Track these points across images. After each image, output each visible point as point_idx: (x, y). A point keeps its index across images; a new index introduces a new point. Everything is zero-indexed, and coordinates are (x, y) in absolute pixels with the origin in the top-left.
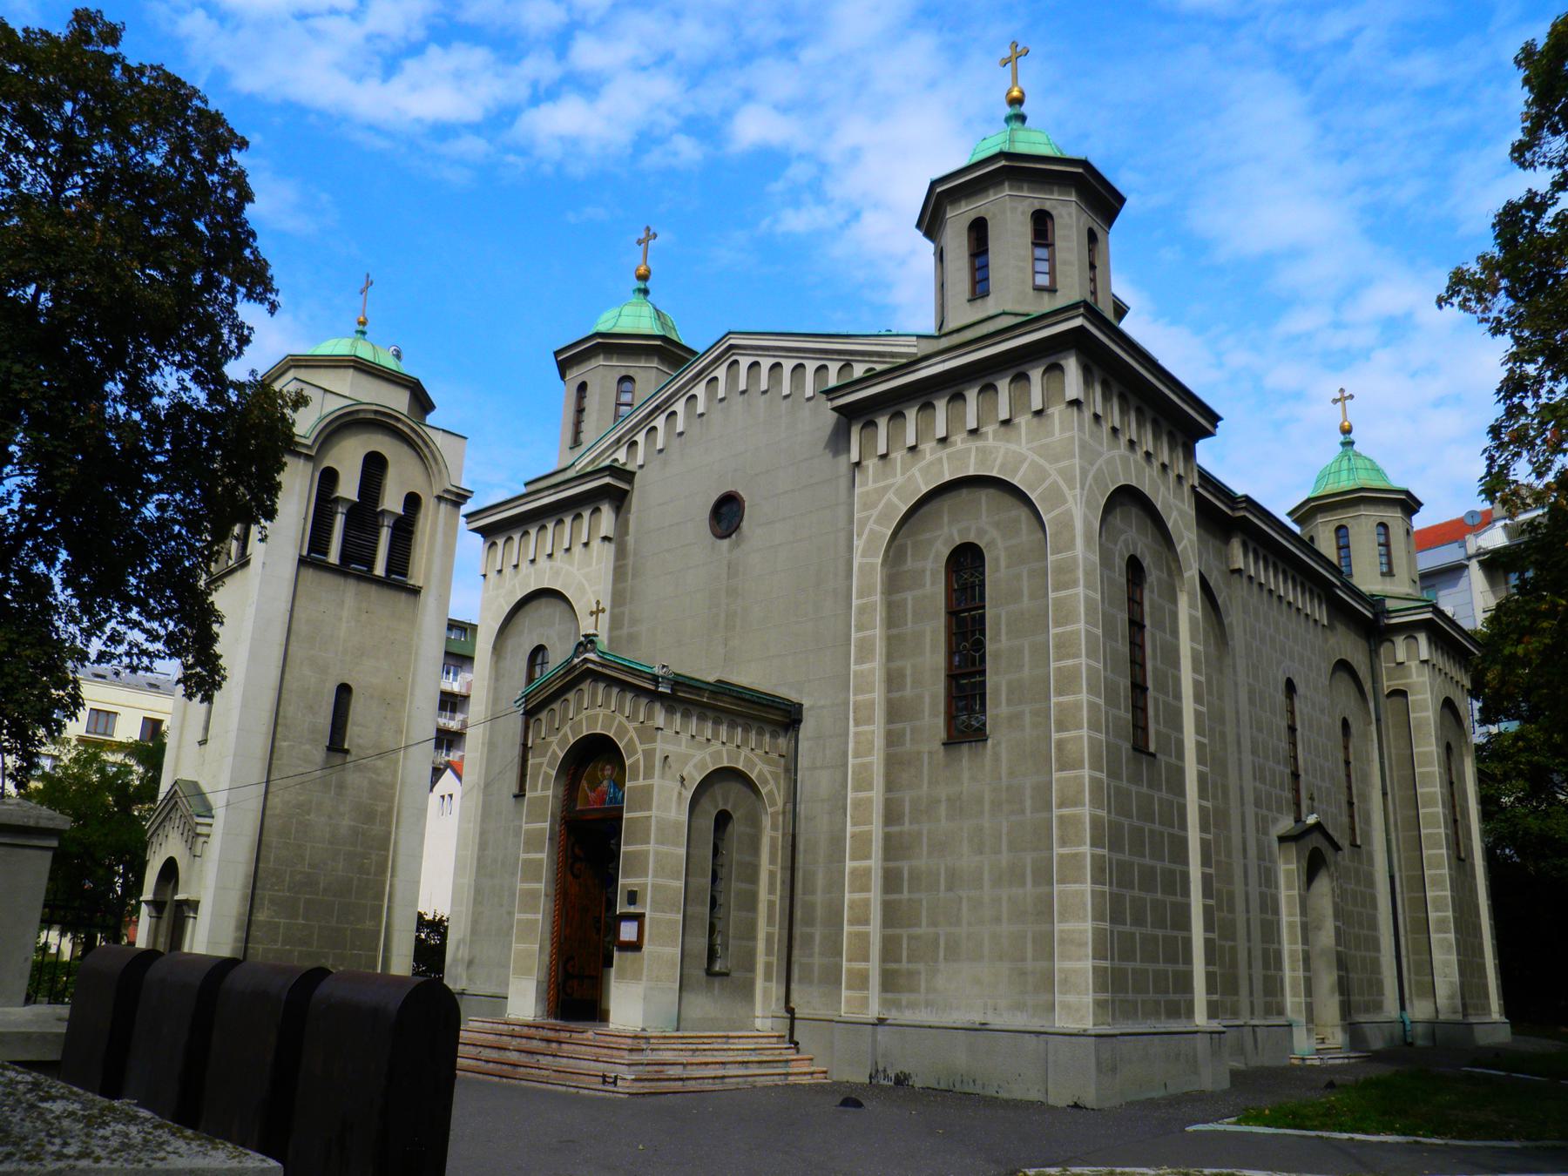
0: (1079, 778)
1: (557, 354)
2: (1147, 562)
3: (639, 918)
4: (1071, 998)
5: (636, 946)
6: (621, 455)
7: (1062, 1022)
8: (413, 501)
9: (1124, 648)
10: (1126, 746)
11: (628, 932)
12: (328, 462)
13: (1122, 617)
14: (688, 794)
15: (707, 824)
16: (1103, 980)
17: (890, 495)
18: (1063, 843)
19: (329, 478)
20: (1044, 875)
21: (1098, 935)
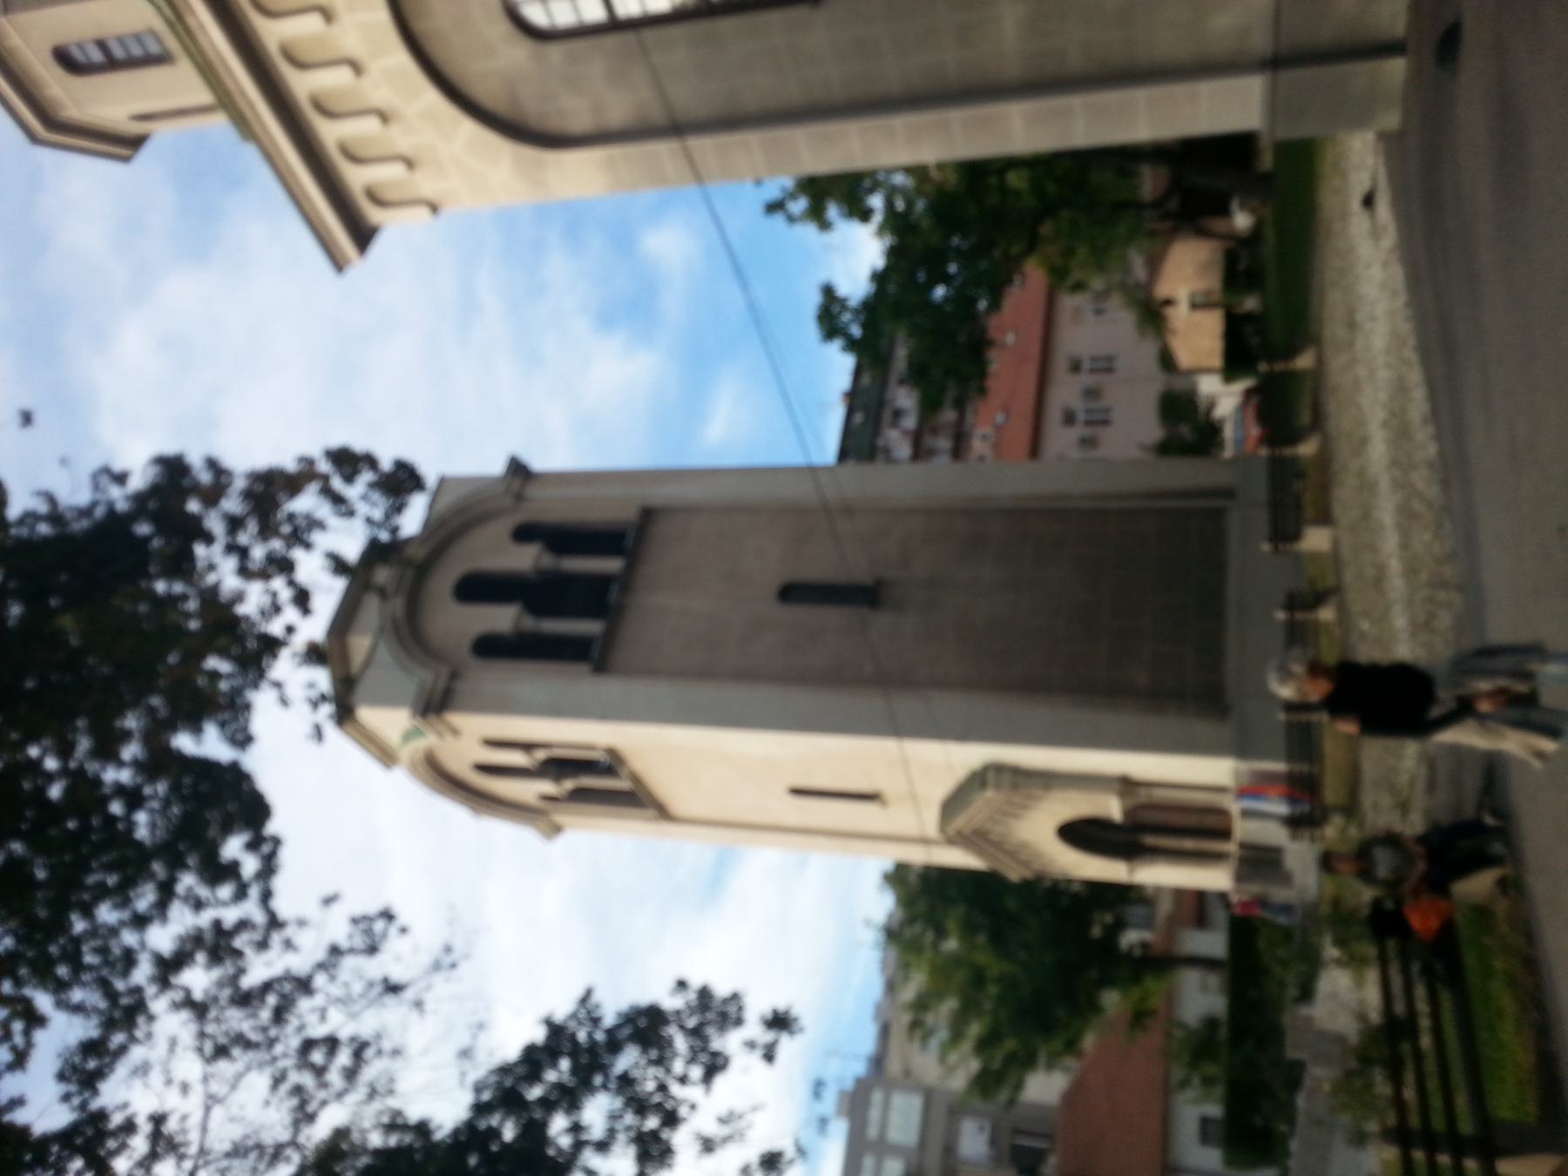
8: (524, 534)
19: (490, 647)
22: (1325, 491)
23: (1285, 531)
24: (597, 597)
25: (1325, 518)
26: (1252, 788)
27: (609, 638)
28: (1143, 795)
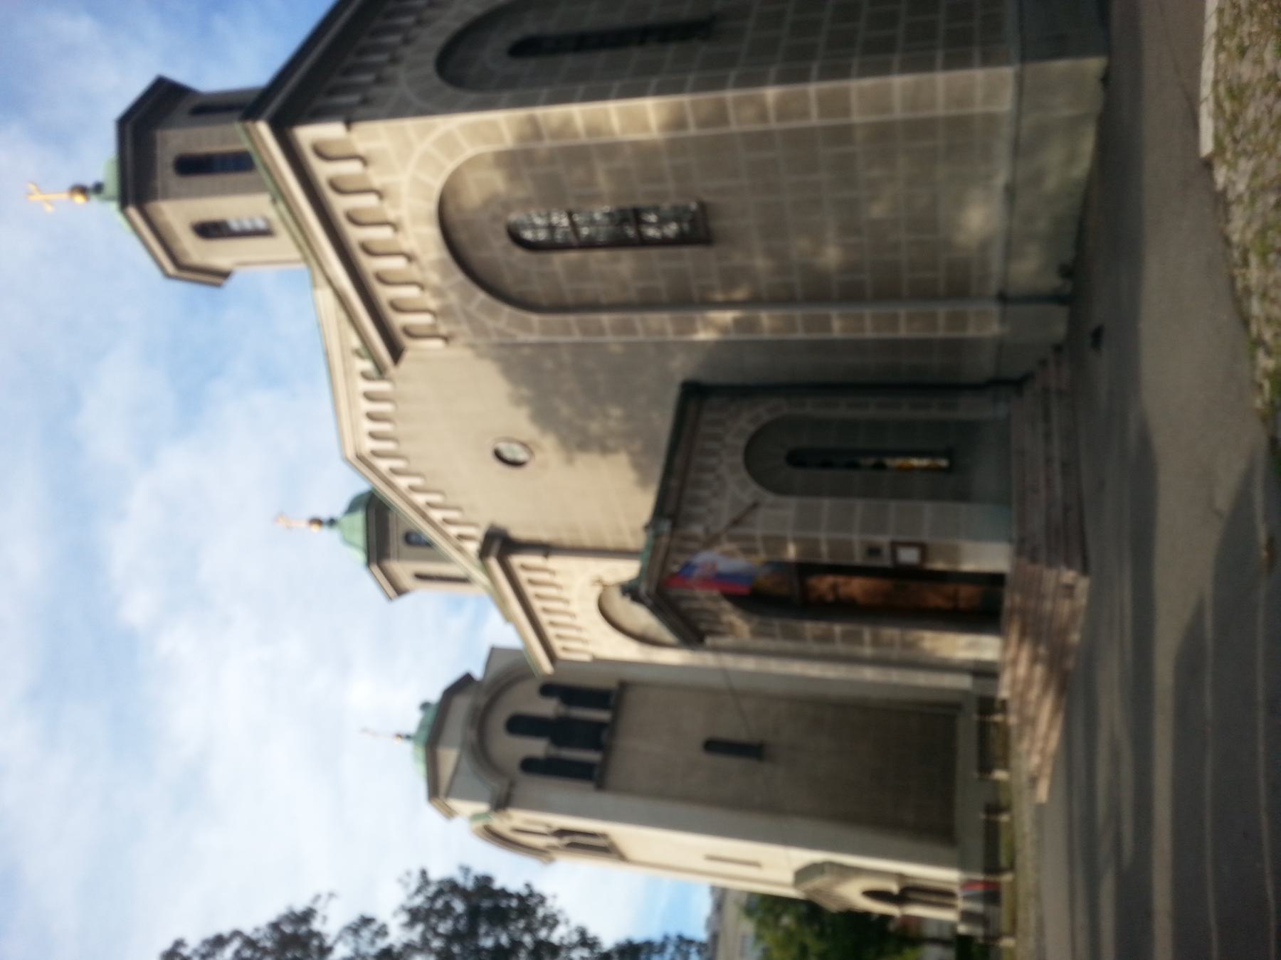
0: (738, 103)
1: (390, 598)
2: (515, 35)
3: (895, 546)
4: (979, 93)
5: (923, 548)
6: (473, 547)
7: (1005, 104)
9: (602, 58)
10: (703, 49)
11: (909, 556)
12: (514, 766)
13: (570, 61)
14: (770, 498)
15: (799, 475)
16: (958, 60)
17: (472, 307)
18: (805, 114)
19: (530, 766)
20: (842, 134)
21: (906, 68)
22: (1006, 746)
23: (985, 767)
24: (596, 736)
25: (1006, 767)
26: (966, 885)
27: (604, 765)
28: (910, 882)
